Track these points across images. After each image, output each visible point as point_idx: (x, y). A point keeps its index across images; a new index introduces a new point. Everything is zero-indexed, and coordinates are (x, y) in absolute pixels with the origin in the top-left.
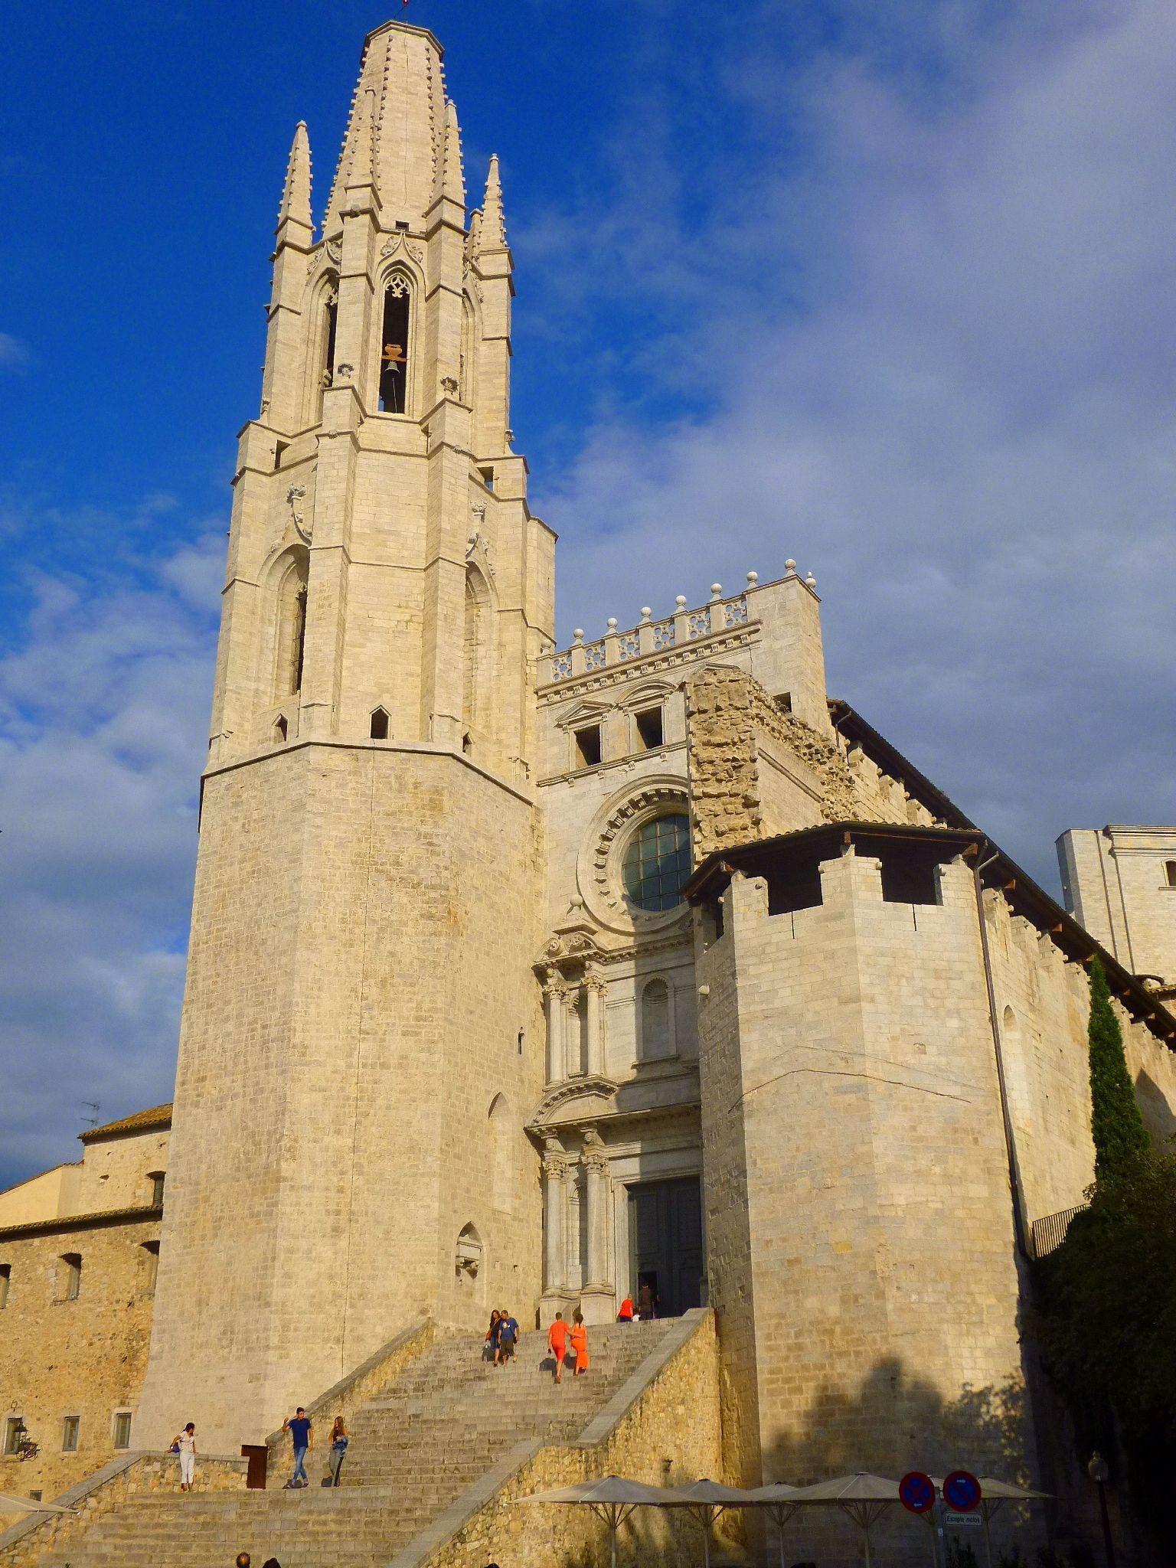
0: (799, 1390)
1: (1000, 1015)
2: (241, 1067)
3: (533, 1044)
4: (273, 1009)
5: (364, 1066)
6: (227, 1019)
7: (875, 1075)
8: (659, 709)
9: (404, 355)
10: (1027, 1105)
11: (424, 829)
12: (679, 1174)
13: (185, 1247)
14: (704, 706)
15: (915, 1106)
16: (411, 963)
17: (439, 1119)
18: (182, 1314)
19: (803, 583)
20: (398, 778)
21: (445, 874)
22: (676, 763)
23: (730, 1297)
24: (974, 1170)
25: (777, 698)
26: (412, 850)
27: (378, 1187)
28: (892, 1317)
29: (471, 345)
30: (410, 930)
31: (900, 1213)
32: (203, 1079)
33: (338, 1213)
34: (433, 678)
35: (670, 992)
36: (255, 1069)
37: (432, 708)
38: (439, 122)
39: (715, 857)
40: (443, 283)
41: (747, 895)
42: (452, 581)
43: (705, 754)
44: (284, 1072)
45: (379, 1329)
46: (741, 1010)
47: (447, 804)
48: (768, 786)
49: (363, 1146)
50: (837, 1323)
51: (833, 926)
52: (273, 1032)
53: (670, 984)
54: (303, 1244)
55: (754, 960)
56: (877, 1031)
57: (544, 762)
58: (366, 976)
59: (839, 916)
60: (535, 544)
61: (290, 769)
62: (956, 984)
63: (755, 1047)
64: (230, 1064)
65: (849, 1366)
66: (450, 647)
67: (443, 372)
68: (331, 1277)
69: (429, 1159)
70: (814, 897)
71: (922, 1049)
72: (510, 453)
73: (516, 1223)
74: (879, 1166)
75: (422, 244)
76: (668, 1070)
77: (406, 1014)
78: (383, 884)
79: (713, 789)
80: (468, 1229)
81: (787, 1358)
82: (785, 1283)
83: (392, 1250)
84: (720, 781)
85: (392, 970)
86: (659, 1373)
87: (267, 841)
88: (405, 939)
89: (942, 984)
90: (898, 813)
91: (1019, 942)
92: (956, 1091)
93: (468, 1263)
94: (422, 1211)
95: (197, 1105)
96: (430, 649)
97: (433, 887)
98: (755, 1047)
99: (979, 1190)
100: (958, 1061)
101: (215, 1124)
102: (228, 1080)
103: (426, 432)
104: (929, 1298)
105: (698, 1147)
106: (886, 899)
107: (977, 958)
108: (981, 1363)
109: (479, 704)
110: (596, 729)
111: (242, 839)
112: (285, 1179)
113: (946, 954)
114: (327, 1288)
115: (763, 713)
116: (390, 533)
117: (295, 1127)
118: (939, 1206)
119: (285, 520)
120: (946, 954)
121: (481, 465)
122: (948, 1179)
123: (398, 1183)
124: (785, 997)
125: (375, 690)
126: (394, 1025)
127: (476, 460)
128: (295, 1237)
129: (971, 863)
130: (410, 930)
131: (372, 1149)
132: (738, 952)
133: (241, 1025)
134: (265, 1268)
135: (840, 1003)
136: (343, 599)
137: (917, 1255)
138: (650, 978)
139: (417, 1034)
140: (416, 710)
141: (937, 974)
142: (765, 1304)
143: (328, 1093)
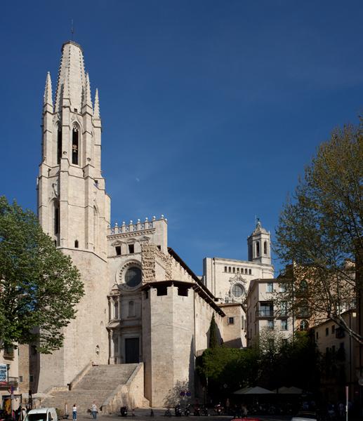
23: (147, 361)
39: (148, 284)
41: (153, 292)
42: (91, 210)
43: (145, 260)
46: (152, 313)
47: (91, 262)
48: (157, 268)
56: (175, 318)
59: (170, 298)
66: (91, 226)
70: (165, 293)
71: (182, 322)
72: (101, 177)
91: (200, 302)
96: (87, 227)
103: (83, 171)
106: (179, 294)
122: (185, 344)
124: (159, 311)
129: (194, 289)
132: (151, 302)
140: (84, 241)
142: (153, 362)
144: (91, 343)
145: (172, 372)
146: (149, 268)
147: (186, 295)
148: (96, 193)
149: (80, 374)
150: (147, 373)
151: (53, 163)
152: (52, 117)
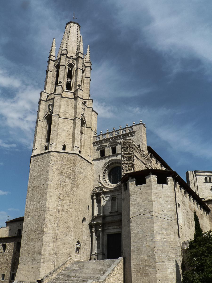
0: (139, 272)
1: (177, 205)
2: (37, 211)
3: (91, 208)
4: (43, 200)
5: (60, 211)
6: (34, 202)
7: (155, 215)
8: (116, 147)
9: (71, 80)
10: (182, 221)
11: (72, 168)
12: (117, 233)
13: (26, 243)
14: (125, 146)
15: (162, 221)
16: (69, 192)
17: (73, 221)
18: (25, 256)
19: (143, 124)
20: (67, 158)
21: (76, 176)
22: (119, 157)
24: (172, 233)
25: (138, 145)
26: (70, 171)
27: (62, 234)
28: (156, 259)
29: (83, 79)
30: (69, 186)
31: (158, 241)
32: (30, 213)
33: (54, 238)
34: (74, 139)
35: (116, 199)
36: (39, 211)
37: (74, 145)
38: (79, 39)
40: (79, 67)
42: (78, 122)
44: (45, 212)
45: (61, 260)
46: (130, 203)
47: (76, 163)
49: (59, 226)
50: (146, 260)
51: (148, 188)
52: (43, 204)
53: (116, 198)
54: (48, 244)
55: (133, 194)
56: (156, 207)
57: (94, 156)
58: (60, 194)
59: (149, 186)
60: (94, 115)
61: (47, 155)
62: (170, 199)
63: (133, 210)
64: (35, 210)
65: (148, 268)
67: (79, 83)
68: (53, 250)
69: (71, 229)
70: (145, 183)
73: (87, 241)
74: (155, 232)
75: (75, 60)
76: (116, 214)
77: (68, 202)
78: (64, 177)
79: (126, 162)
80: (78, 242)
81: (137, 266)
82: (137, 253)
83: (64, 245)
84: (127, 161)
85: (65, 194)
86: (114, 269)
87: (43, 169)
88: (68, 188)
89: (167, 199)
90: (159, 167)
92: (169, 218)
93: (78, 248)
94: (70, 238)
95: (28, 217)
97: (73, 178)
98: (133, 210)
99: (173, 237)
100: (170, 213)
101: (32, 221)
102: (34, 213)
103: (74, 95)
104: (163, 256)
105: (121, 228)
107: (173, 194)
108: (172, 267)
109: (83, 145)
110: (104, 150)
111: (38, 168)
112: (45, 232)
113: (168, 194)
114: (52, 252)
115: (136, 148)
116: (67, 112)
117: (46, 222)
118: (165, 239)
119: (48, 110)
120: (168, 194)
121: (84, 101)
122: (167, 234)
123: (65, 233)
124: (139, 201)
125: (63, 141)
126: (65, 204)
127: (83, 100)
128: (46, 242)
130: (69, 186)
131: (61, 227)
133: (37, 203)
134: (41, 248)
135: (149, 202)
136: (58, 124)
137: (161, 248)
138: (113, 197)
139: (69, 206)
140: (71, 145)
141: (166, 197)
142: (133, 256)
143: (53, 216)
144: (70, 239)
145: (154, 267)
146: (128, 162)
147: (166, 183)
148: (84, 109)
149: (54, 271)
150: (126, 266)
151: (51, 91)
152: (53, 63)
